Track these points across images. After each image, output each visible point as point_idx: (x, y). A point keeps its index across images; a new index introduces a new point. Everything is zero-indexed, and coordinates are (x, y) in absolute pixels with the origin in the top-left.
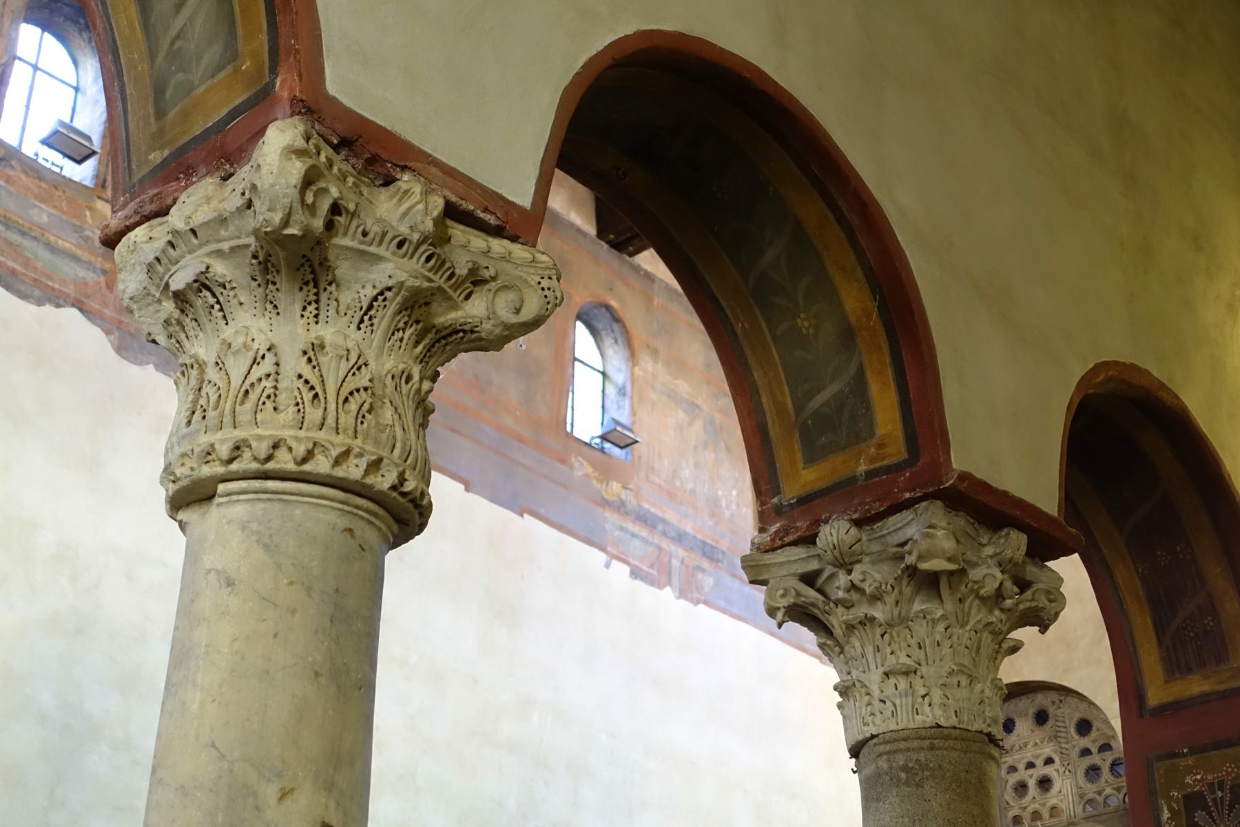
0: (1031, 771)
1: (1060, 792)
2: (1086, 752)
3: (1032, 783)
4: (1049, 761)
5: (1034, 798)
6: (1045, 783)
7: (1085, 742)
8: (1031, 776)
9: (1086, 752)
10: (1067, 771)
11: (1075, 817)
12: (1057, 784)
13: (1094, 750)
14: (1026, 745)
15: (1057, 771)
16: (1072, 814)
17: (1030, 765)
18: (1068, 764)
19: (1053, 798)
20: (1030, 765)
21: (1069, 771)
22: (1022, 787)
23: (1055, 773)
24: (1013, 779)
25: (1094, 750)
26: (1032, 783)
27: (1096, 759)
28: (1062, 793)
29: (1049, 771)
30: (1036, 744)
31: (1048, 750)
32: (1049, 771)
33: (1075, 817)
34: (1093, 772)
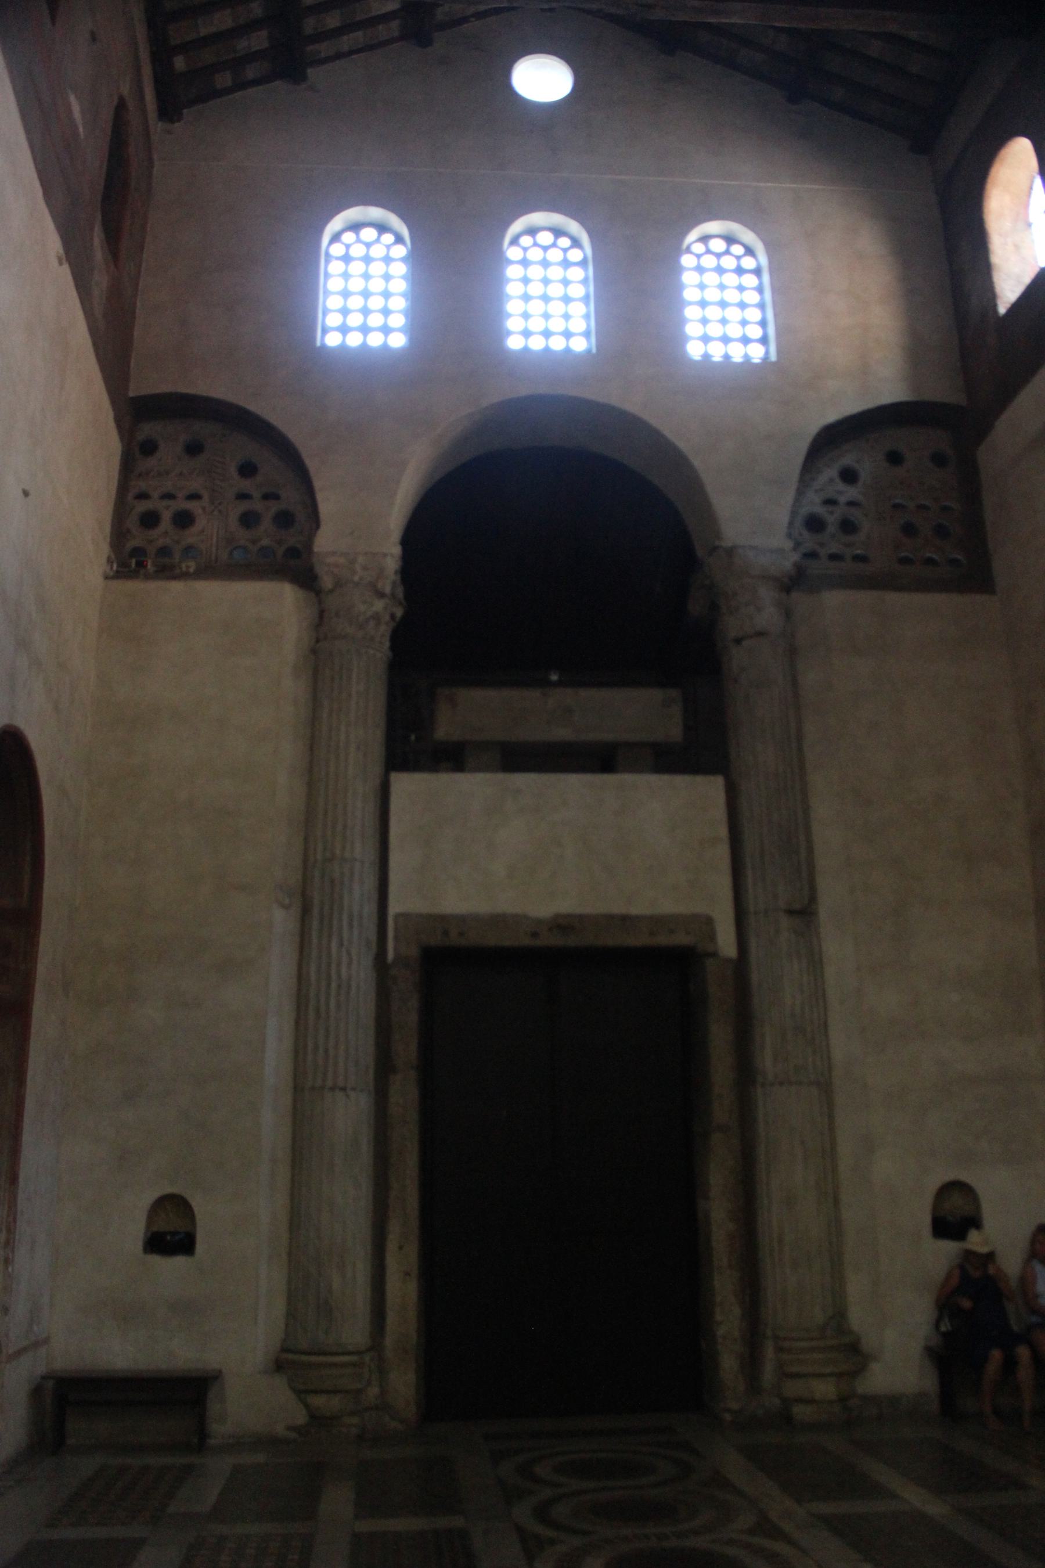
0: (171, 503)
1: (203, 532)
2: (243, 496)
3: (166, 516)
4: (194, 497)
5: (166, 533)
6: (184, 520)
7: (245, 485)
8: (167, 508)
9: (243, 496)
10: (216, 513)
11: (216, 562)
12: (201, 522)
13: (256, 494)
14: (167, 473)
15: (204, 509)
16: (213, 558)
17: (169, 496)
18: (220, 504)
19: (191, 536)
20: (169, 496)
21: (220, 511)
22: (150, 520)
23: (200, 511)
24: (142, 507)
25: (256, 494)
26: (166, 516)
27: (258, 505)
28: (205, 533)
29: (193, 506)
30: (181, 474)
31: (196, 484)
32: (193, 506)
33: (216, 562)
34: (248, 520)
